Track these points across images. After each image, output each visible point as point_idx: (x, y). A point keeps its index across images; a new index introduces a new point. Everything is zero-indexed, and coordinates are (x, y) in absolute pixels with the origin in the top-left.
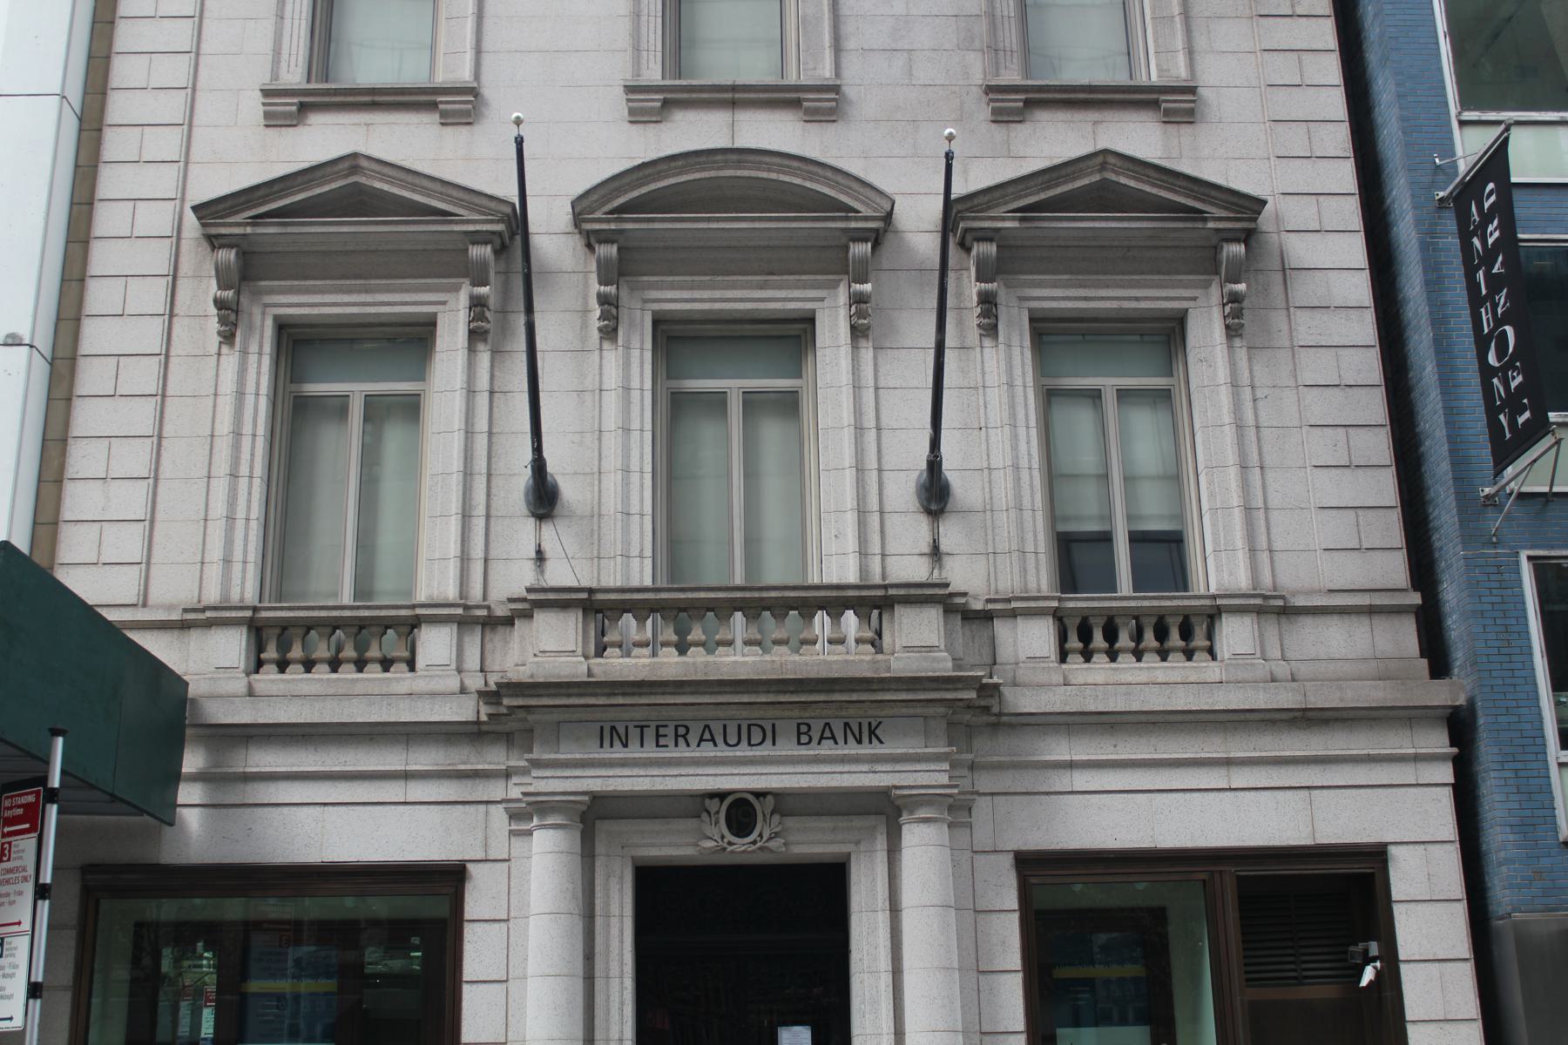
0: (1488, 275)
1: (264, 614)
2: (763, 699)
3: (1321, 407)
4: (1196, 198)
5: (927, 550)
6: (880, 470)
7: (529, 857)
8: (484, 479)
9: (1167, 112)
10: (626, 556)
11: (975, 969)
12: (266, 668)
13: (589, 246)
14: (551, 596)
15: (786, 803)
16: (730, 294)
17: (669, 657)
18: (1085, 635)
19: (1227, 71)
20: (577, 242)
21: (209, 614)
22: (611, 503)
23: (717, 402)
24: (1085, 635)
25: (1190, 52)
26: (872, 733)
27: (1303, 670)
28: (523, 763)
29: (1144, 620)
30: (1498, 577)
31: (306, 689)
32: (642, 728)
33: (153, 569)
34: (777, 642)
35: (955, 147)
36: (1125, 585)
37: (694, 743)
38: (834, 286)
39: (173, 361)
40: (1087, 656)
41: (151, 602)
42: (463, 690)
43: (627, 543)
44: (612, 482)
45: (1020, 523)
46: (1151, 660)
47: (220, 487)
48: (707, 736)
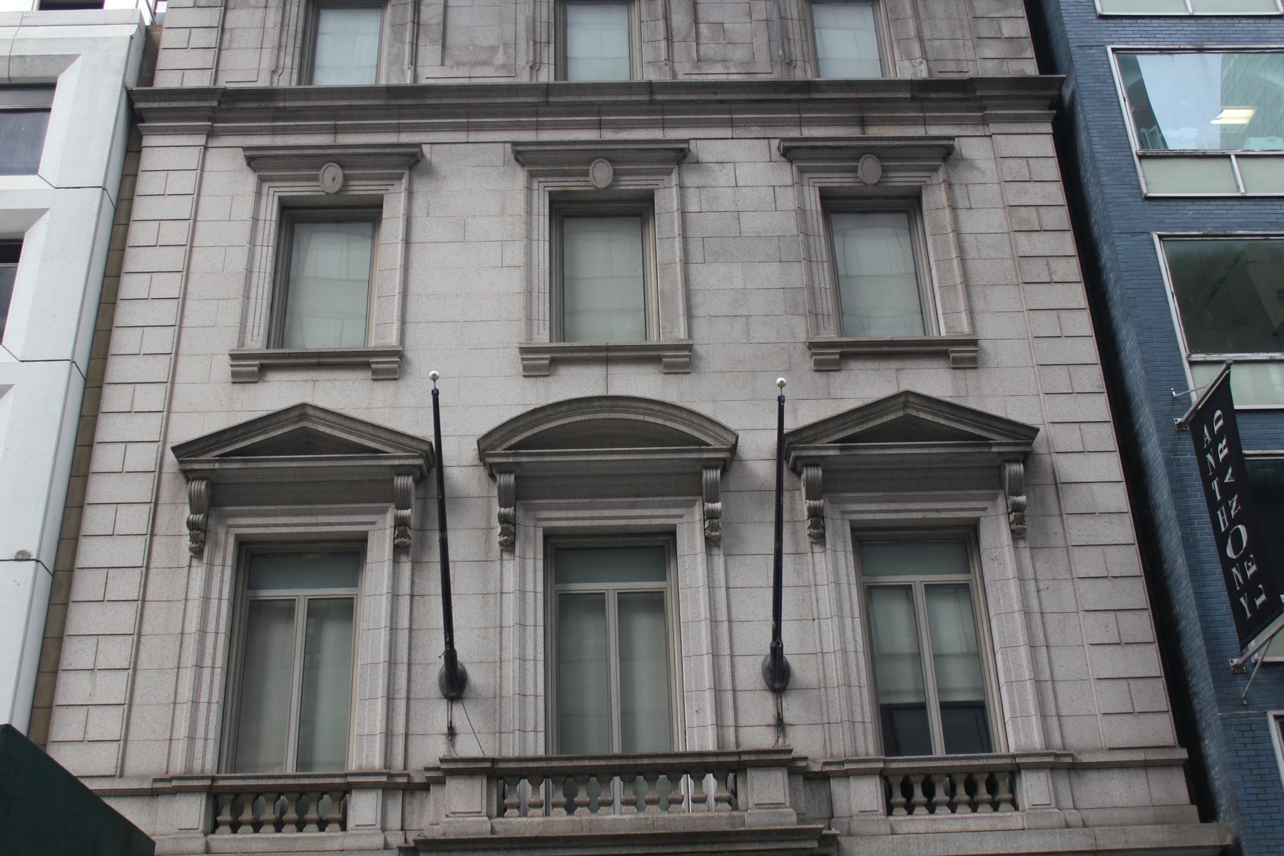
0: (1221, 484)
1: (221, 783)
3: (1094, 595)
4: (982, 428)
5: (773, 721)
6: (732, 656)
8: (405, 668)
9: (955, 360)
10: (523, 731)
12: (221, 829)
13: (492, 476)
14: (461, 766)
17: (559, 816)
18: (907, 791)
19: (999, 329)
20: (482, 472)
21: (175, 783)
22: (510, 686)
23: (596, 603)
24: (907, 791)
27: (1092, 817)
30: (1250, 734)
33: (130, 746)
34: (650, 802)
35: (785, 392)
36: (939, 748)
38: (690, 505)
39: (153, 572)
41: (128, 771)
42: (386, 846)
43: (523, 719)
44: (511, 669)
45: (849, 697)
46: (963, 812)
47: (187, 676)
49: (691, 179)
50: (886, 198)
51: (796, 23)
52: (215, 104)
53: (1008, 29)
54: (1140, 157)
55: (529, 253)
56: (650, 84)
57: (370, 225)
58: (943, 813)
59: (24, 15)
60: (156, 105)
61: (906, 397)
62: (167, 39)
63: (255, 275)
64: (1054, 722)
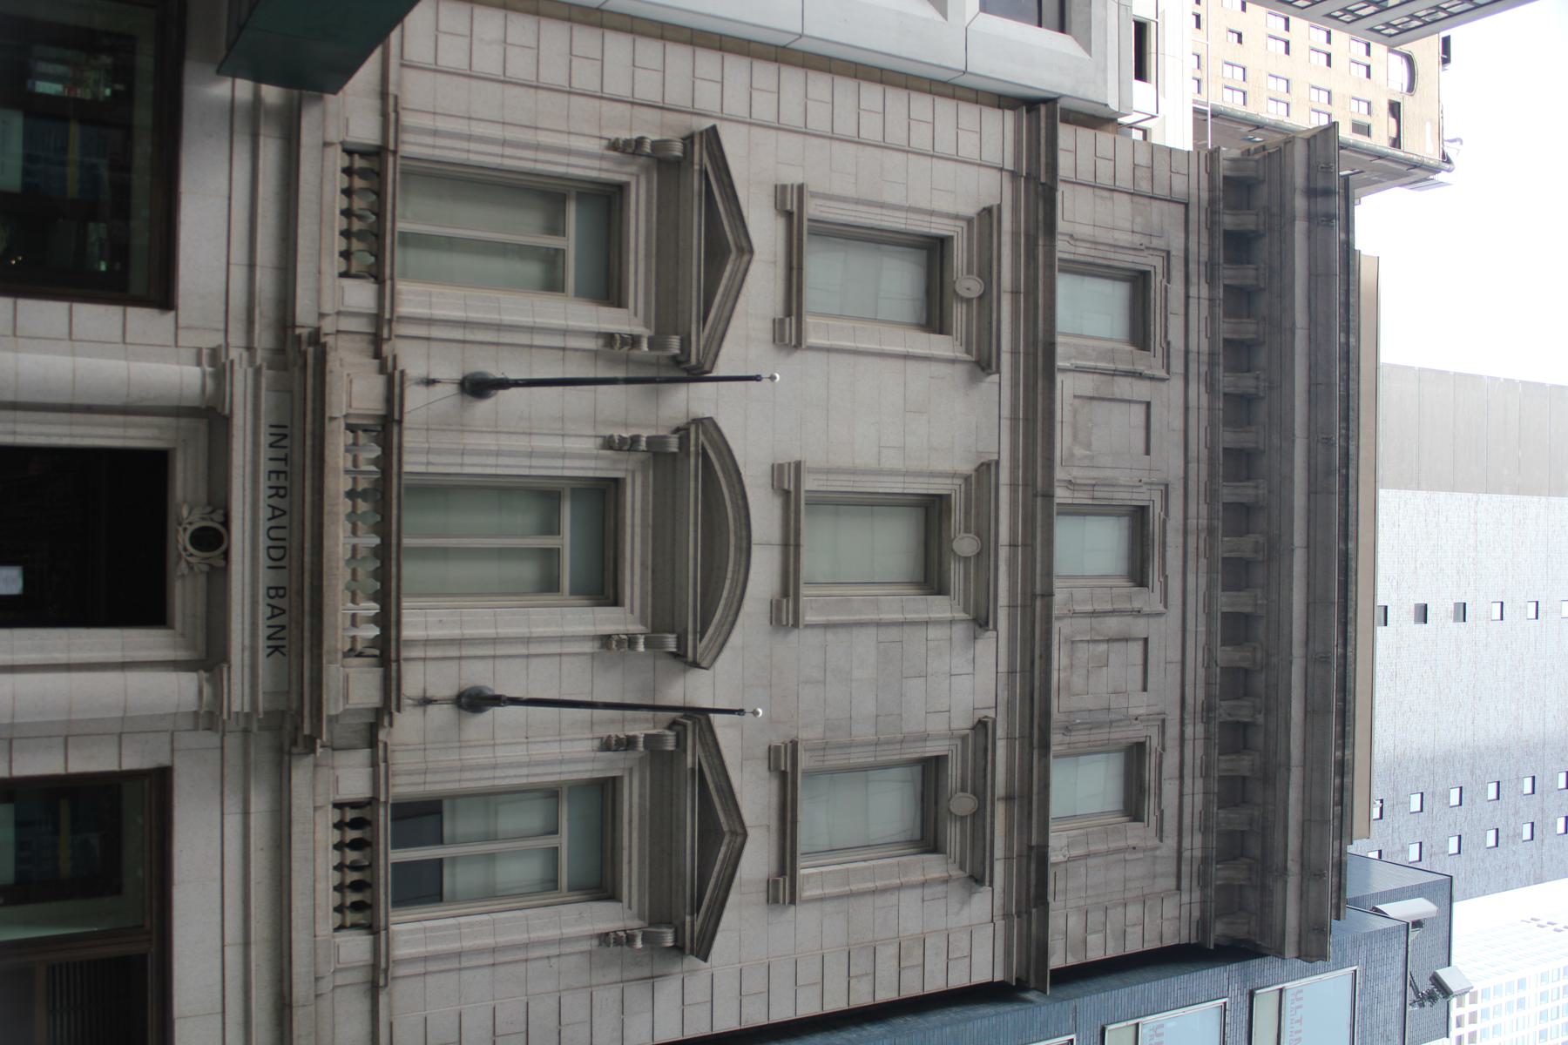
1: (391, 159)
2: (307, 559)
3: (543, 1011)
5: (429, 694)
6: (494, 657)
7: (178, 363)
9: (776, 882)
10: (429, 451)
11: (68, 734)
12: (346, 158)
13: (677, 430)
14: (397, 390)
15: (218, 576)
17: (344, 484)
18: (356, 824)
19: (804, 927)
20: (681, 421)
21: (392, 116)
22: (472, 441)
23: (551, 528)
24: (356, 824)
25: (822, 899)
26: (276, 648)
28: (259, 361)
29: (368, 872)
31: (328, 188)
32: (285, 460)
33: (431, 75)
34: (354, 572)
35: (748, 717)
36: (396, 855)
38: (643, 622)
39: (597, 102)
40: (339, 826)
42: (322, 316)
43: (439, 452)
44: (489, 442)
45: (450, 770)
46: (335, 878)
47: (495, 131)
48: (277, 513)
49: (959, 632)
50: (936, 819)
51: (1105, 736)
52: (1043, 180)
53: (1094, 940)
55: (893, 473)
56: (1051, 595)
57: (924, 321)
58: (334, 857)
59: (1129, 8)
60: (1043, 125)
62: (1104, 138)
64: (419, 969)
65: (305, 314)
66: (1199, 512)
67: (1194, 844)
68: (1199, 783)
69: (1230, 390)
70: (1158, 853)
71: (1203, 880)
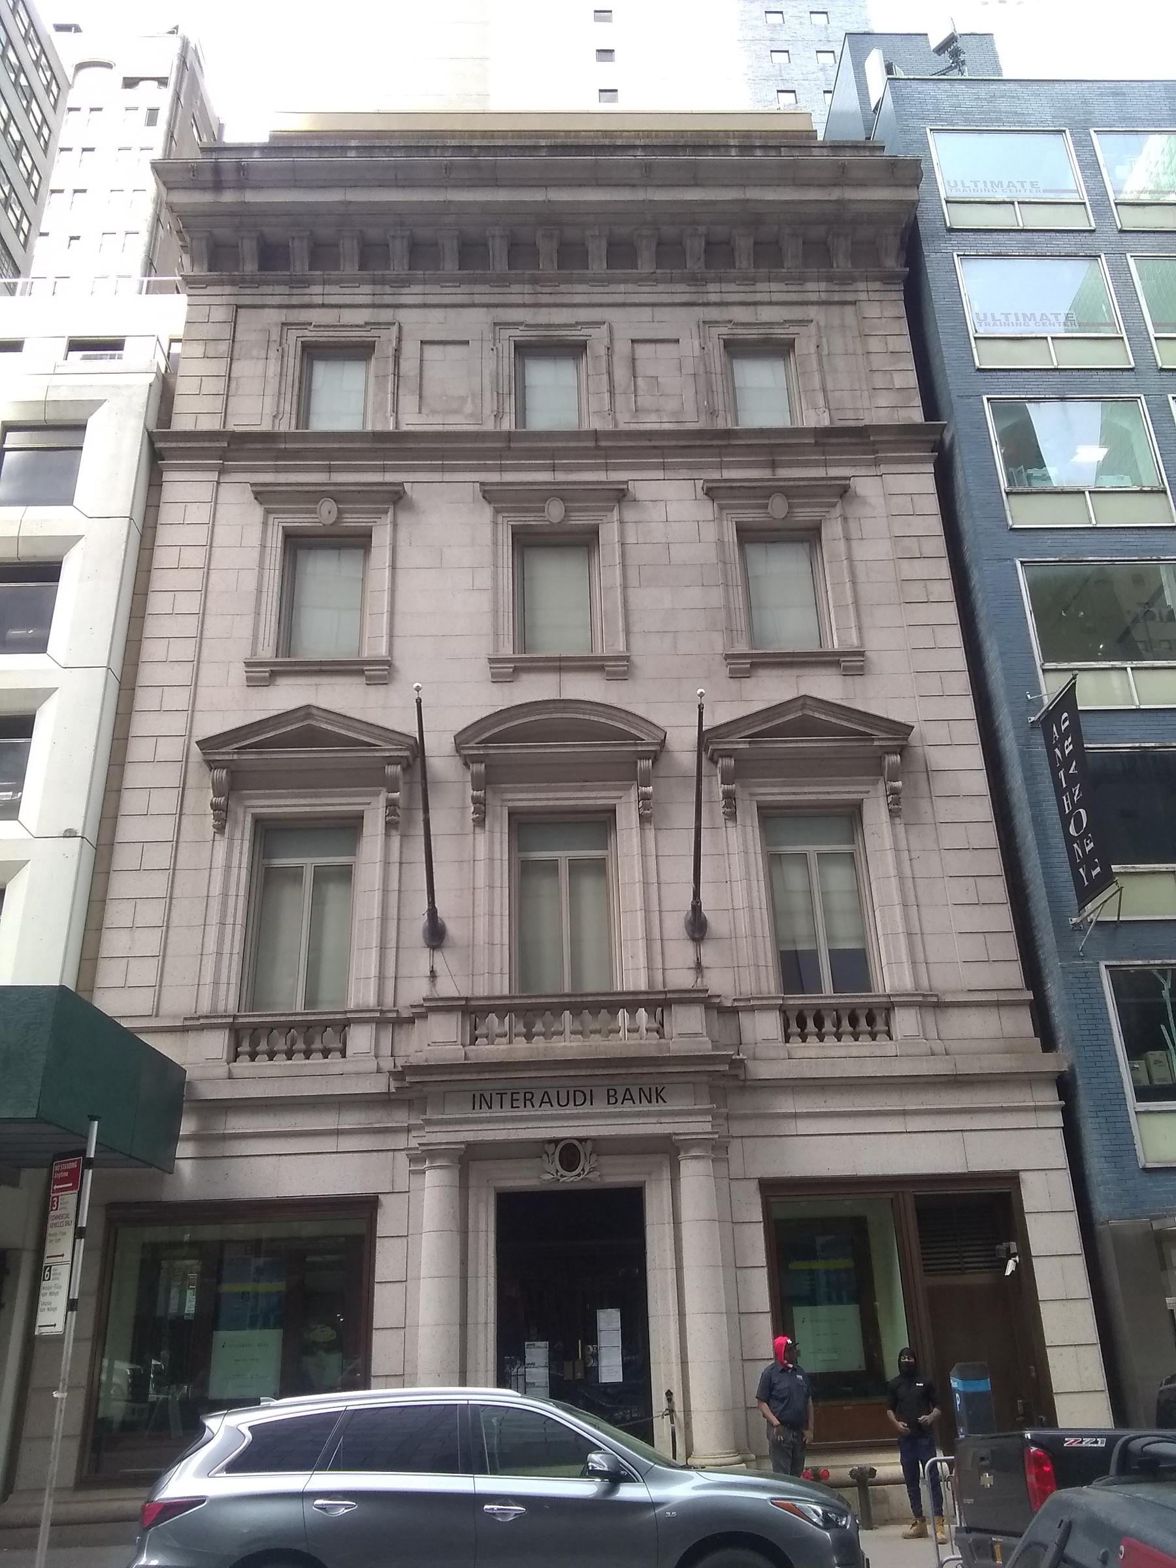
1: (241, 1020)
6: (660, 912)
9: (845, 668)
10: (491, 973)
11: (733, 1266)
13: (466, 765)
14: (440, 1003)
15: (601, 1146)
16: (559, 795)
17: (520, 1043)
18: (802, 1023)
19: (884, 642)
20: (458, 761)
21: (202, 1021)
22: (481, 938)
23: (551, 867)
24: (802, 1023)
25: (860, 629)
26: (658, 1095)
27: (954, 1046)
30: (1086, 980)
31: (268, 1073)
34: (592, 1032)
36: (827, 990)
37: (537, 1104)
38: (628, 788)
39: (182, 846)
42: (379, 1071)
43: (491, 964)
44: (482, 923)
45: (755, 947)
46: (847, 1040)
48: (546, 1099)
49: (630, 515)
50: (792, 530)
51: (719, 377)
52: (226, 445)
53: (899, 381)
54: (1007, 494)
55: (495, 578)
58: (830, 1041)
60: (174, 445)
61: (804, 701)
62: (183, 386)
63: (264, 595)
65: (378, 1085)
66: (518, 292)
67: (815, 289)
68: (760, 286)
69: (406, 261)
70: (822, 324)
71: (847, 280)
